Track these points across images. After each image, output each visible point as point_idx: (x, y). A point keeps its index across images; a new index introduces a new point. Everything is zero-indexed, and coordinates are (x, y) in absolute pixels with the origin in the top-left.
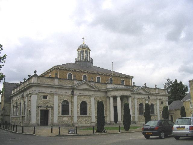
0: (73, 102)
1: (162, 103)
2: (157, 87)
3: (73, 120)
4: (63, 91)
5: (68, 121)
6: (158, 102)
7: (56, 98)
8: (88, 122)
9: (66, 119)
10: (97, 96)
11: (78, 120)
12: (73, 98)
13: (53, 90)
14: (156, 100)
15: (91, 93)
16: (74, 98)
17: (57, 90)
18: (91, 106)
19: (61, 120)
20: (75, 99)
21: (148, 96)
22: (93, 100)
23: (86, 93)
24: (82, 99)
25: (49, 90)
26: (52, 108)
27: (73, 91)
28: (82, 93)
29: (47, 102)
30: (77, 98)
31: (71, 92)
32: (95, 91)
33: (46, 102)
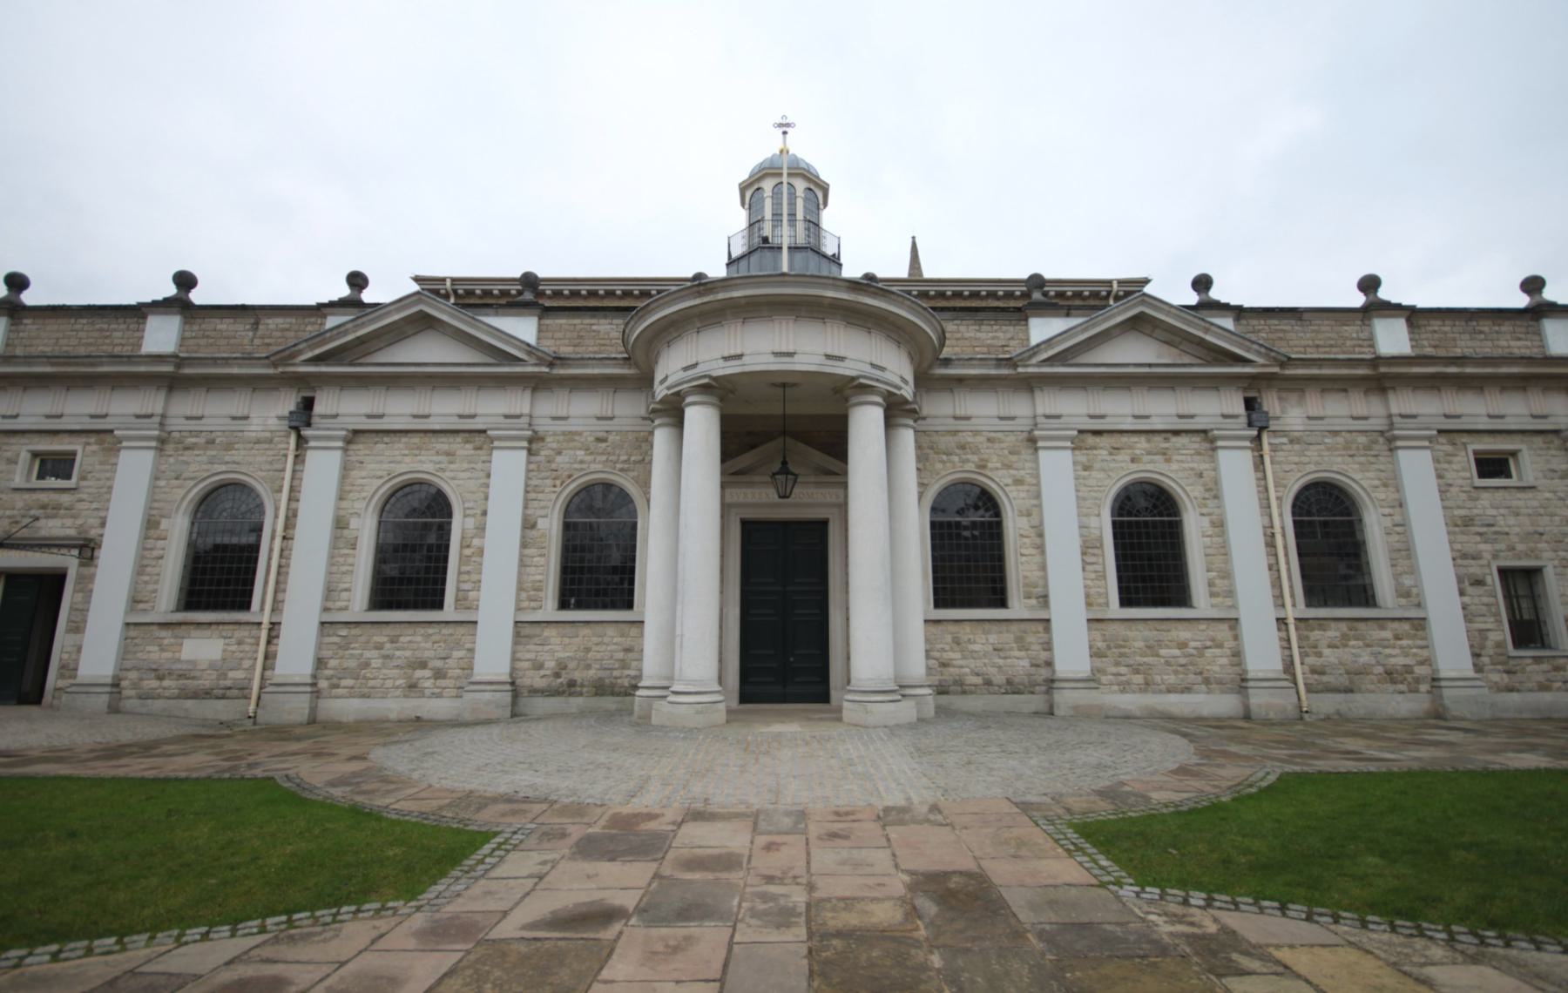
0: (294, 497)
1: (1493, 466)
2: (1384, 294)
3: (269, 657)
4: (216, 409)
5: (220, 668)
6: (1416, 466)
7: (134, 470)
8: (439, 674)
9: (205, 647)
10: (561, 427)
11: (320, 663)
12: (299, 459)
13: (122, 406)
14: (1389, 439)
15: (491, 407)
16: (311, 456)
17: (151, 402)
18: (481, 529)
19: (153, 654)
20: (323, 466)
21: (1250, 404)
22: (509, 466)
23: (445, 408)
24: (388, 466)
25: (78, 408)
26: (87, 549)
27: (308, 404)
28: (399, 408)
29: (57, 507)
30: (339, 454)
31: (287, 403)
32: (537, 384)
33: (44, 507)
